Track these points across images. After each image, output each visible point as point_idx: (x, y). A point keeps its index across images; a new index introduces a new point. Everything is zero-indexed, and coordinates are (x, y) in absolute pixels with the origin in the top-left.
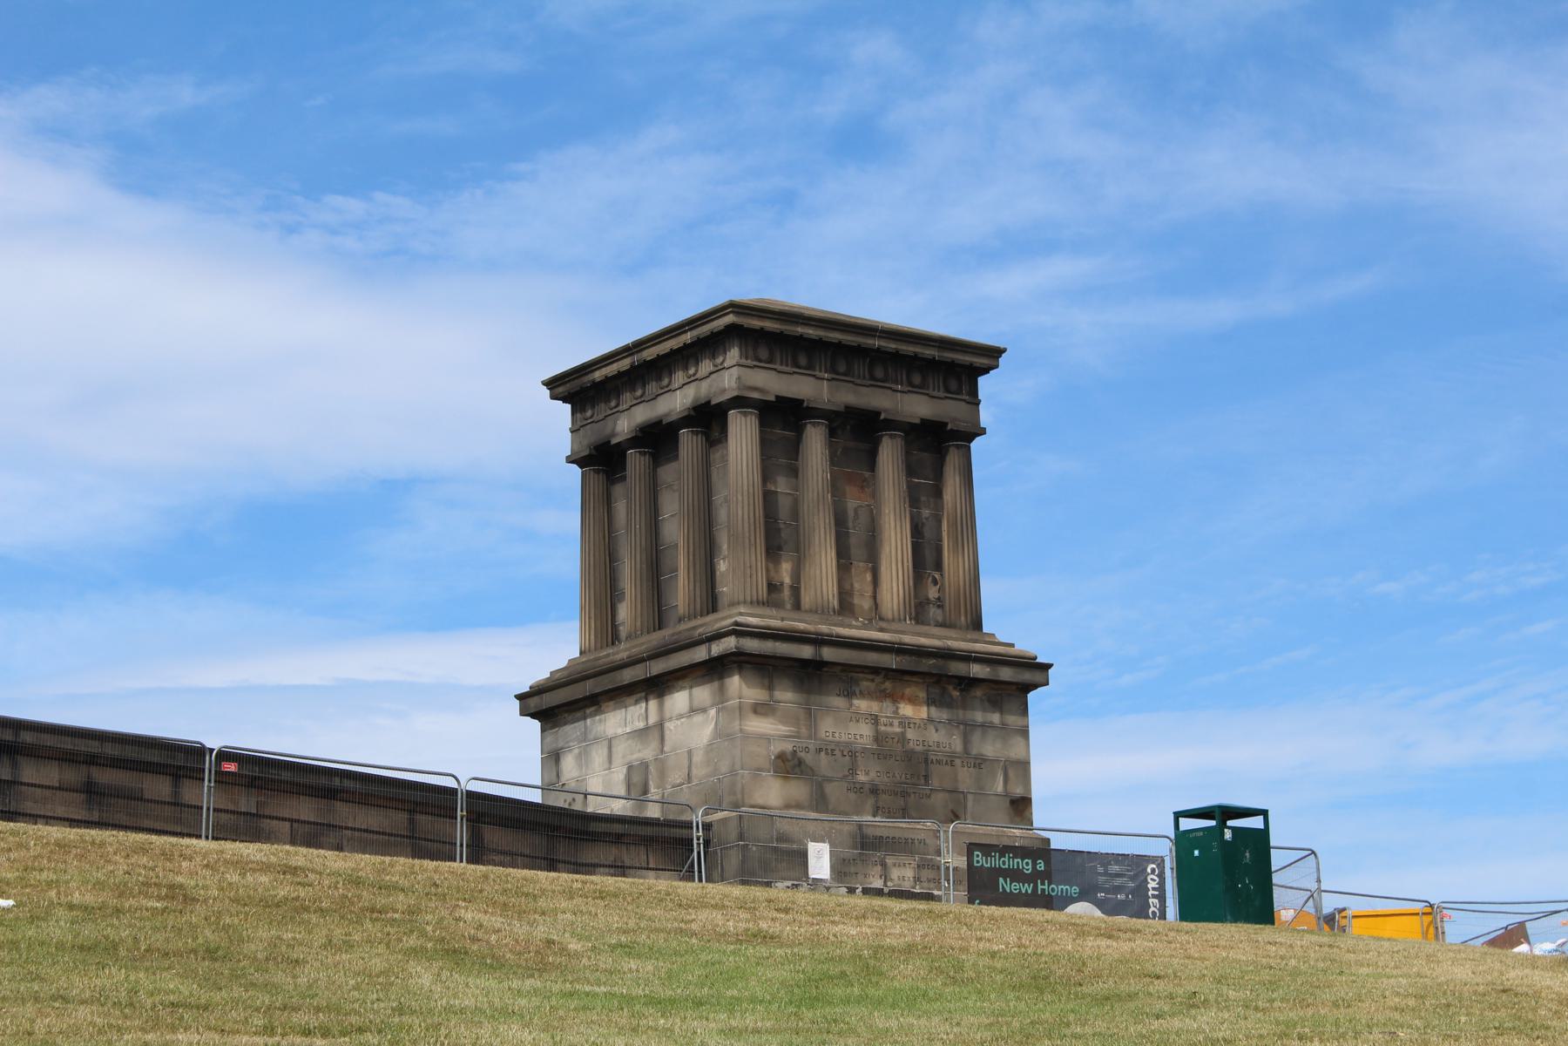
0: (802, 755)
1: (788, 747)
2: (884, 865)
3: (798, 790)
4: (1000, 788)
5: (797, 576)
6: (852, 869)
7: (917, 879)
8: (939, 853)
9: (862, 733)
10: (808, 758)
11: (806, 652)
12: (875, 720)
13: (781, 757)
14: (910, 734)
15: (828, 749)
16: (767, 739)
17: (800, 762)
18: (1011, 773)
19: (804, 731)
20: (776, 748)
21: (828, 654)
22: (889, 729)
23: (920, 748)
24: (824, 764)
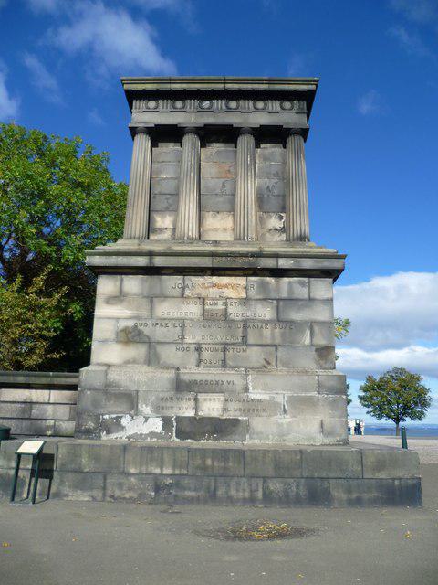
0: (142, 328)
1: (131, 323)
2: (196, 400)
3: (138, 351)
4: (307, 341)
5: (175, 223)
6: (169, 404)
7: (225, 410)
8: (247, 390)
9: (193, 310)
10: (146, 331)
11: (141, 261)
12: (202, 300)
13: (125, 330)
14: (231, 310)
15: (163, 322)
16: (117, 319)
17: (140, 333)
18: (316, 329)
19: (145, 313)
20: (123, 324)
21: (158, 261)
22: (214, 307)
23: (240, 318)
24: (159, 333)
